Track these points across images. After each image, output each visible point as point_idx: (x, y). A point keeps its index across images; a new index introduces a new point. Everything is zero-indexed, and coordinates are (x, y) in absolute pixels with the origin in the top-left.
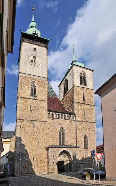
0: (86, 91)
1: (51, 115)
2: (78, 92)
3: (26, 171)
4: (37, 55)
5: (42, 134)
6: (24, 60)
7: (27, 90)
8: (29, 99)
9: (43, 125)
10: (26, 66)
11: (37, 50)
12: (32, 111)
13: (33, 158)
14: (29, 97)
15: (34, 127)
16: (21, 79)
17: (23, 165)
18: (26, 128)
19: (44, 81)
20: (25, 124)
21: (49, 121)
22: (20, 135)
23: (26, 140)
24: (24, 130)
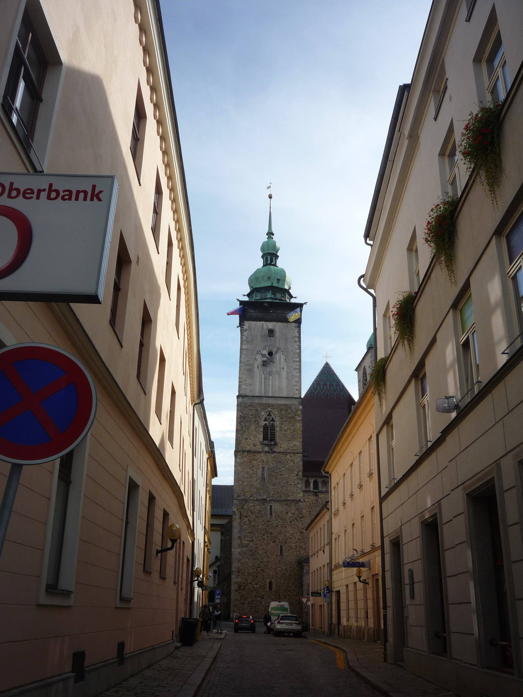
1: (312, 485)
5: (289, 529)
6: (248, 365)
7: (254, 433)
8: (258, 452)
9: (293, 508)
10: (252, 377)
11: (277, 334)
12: (266, 480)
13: (270, 583)
14: (259, 448)
15: (271, 514)
16: (241, 411)
17: (246, 598)
19: (293, 407)
21: (307, 500)
23: (252, 544)
24: (249, 521)
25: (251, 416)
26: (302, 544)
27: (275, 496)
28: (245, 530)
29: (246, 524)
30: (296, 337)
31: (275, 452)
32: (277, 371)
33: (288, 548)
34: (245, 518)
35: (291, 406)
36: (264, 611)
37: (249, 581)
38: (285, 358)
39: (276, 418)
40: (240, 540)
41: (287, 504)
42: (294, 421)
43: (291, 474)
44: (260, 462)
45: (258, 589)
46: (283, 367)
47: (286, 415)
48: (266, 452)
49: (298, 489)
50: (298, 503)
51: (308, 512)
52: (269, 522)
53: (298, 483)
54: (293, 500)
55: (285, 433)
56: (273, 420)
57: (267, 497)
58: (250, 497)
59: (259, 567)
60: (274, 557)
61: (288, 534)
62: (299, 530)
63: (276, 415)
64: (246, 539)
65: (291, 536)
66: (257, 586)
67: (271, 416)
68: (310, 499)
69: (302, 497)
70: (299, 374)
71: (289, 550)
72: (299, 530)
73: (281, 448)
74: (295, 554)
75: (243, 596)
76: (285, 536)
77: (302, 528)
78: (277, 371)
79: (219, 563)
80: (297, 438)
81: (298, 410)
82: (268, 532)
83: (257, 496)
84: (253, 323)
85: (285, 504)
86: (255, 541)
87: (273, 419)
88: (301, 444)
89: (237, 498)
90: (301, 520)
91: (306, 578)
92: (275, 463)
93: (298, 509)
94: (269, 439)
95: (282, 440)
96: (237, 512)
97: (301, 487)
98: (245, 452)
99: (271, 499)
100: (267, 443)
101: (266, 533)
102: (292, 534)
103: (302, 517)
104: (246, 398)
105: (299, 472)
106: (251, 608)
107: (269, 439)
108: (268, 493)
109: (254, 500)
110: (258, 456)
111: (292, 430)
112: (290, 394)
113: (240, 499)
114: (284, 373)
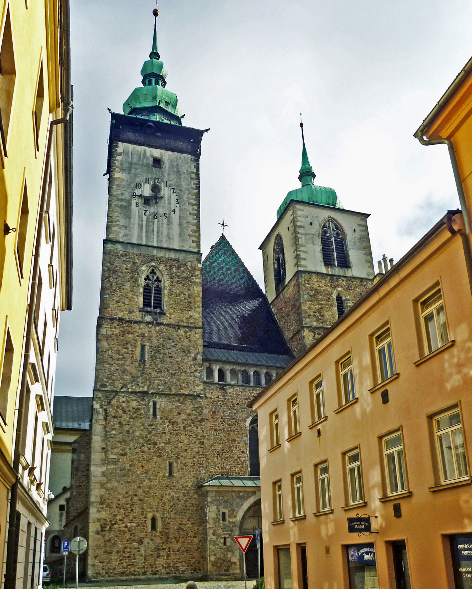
0: (348, 288)
2: (317, 292)
3: (125, 565)
4: (165, 179)
5: (182, 436)
6: (122, 200)
7: (130, 295)
9: (189, 407)
11: (166, 165)
12: (148, 365)
13: (154, 520)
14: (137, 316)
15: (155, 415)
18: (127, 419)
19: (189, 264)
20: (124, 405)
21: (209, 395)
22: (103, 441)
25: (126, 270)
26: (203, 459)
27: (162, 388)
28: (112, 437)
29: (115, 429)
30: (193, 173)
31: (162, 324)
32: (166, 214)
33: (182, 466)
34: (113, 419)
35: (186, 263)
36: (144, 563)
37: (119, 517)
38: (176, 197)
39: (163, 276)
40: (105, 452)
41: (179, 400)
42: (190, 283)
43: (186, 357)
44: (138, 336)
45: (133, 528)
46: (174, 210)
47: (179, 274)
48: (148, 323)
49: (196, 379)
50: (196, 399)
51: (211, 413)
52: (151, 425)
53: (196, 371)
54: (189, 395)
55: (177, 299)
56: (158, 280)
57: (148, 388)
58: (122, 388)
59: (135, 495)
60: (159, 480)
61: (180, 445)
62: (198, 439)
63: (163, 272)
64: (115, 451)
65: (186, 448)
66: (132, 524)
67: (155, 274)
68: (214, 394)
69: (202, 390)
70: (197, 221)
71: (182, 469)
72: (198, 439)
73: (170, 318)
74: (192, 475)
75: (109, 541)
76: (176, 448)
77: (202, 436)
78: (166, 214)
79: (68, 495)
80: (195, 308)
81: (195, 269)
82: (149, 440)
83: (132, 386)
84: (131, 147)
85: (177, 399)
86: (129, 454)
87: (158, 278)
88: (201, 315)
89: (101, 389)
90: (200, 425)
91: (211, 510)
92: (161, 340)
93: (195, 409)
94: (153, 305)
95: (172, 307)
96: (101, 410)
97: (201, 376)
98: (115, 321)
99: (154, 391)
100: (149, 309)
101: (146, 442)
102: (188, 444)
103: (202, 420)
104: (119, 246)
105: (198, 353)
106: (122, 560)
107: (153, 305)
108: (150, 382)
109: (128, 392)
110: (136, 327)
111: (187, 295)
112: (183, 246)
113: (106, 391)
114: (175, 218)
